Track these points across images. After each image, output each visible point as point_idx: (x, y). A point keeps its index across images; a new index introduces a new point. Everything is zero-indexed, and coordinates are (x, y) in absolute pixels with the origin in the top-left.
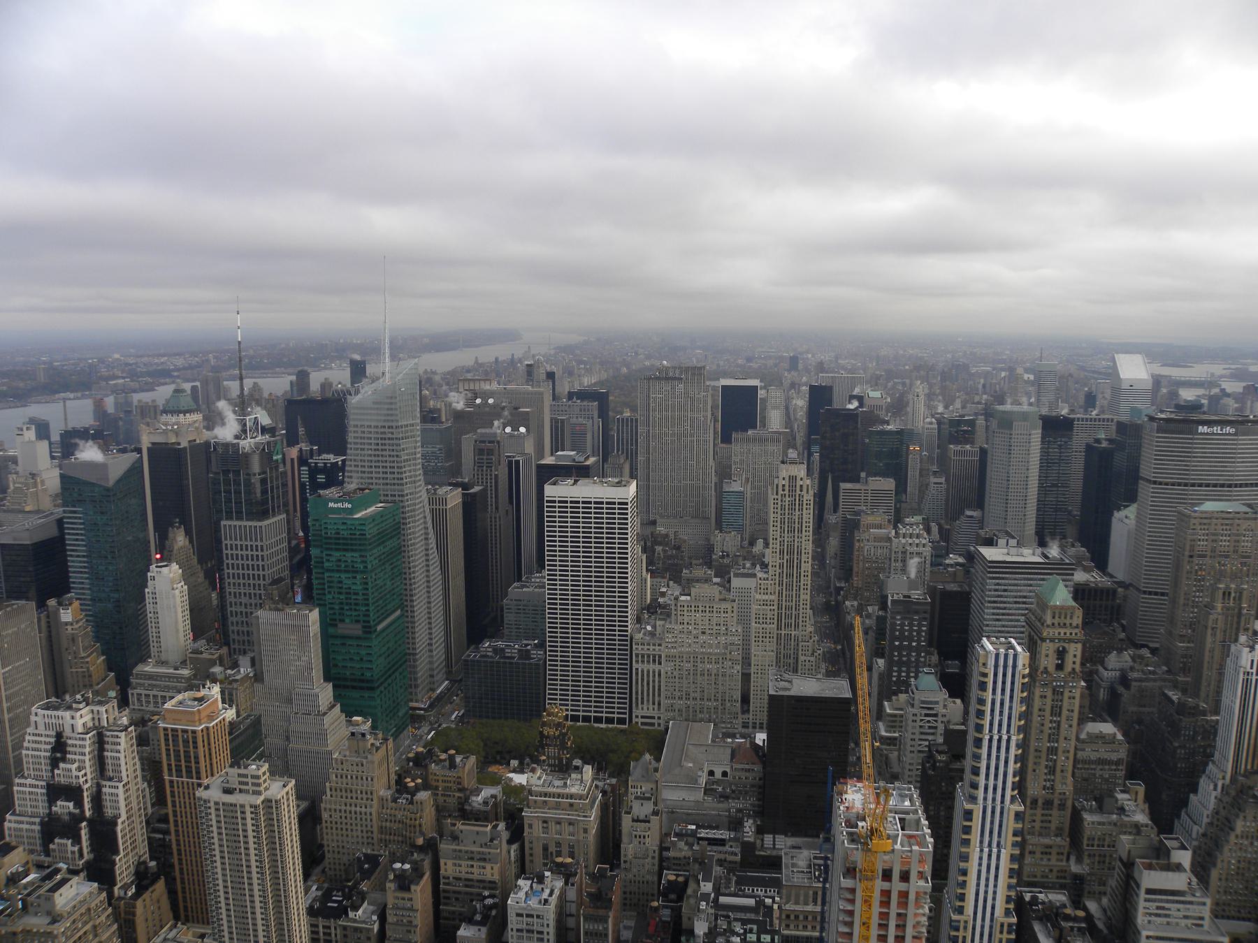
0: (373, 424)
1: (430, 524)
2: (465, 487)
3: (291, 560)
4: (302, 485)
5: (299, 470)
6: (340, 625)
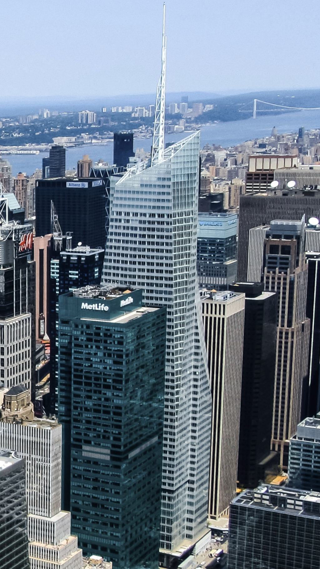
0: (148, 211)
1: (201, 337)
2: (251, 291)
3: (33, 367)
4: (51, 282)
5: (49, 264)
6: (85, 447)
